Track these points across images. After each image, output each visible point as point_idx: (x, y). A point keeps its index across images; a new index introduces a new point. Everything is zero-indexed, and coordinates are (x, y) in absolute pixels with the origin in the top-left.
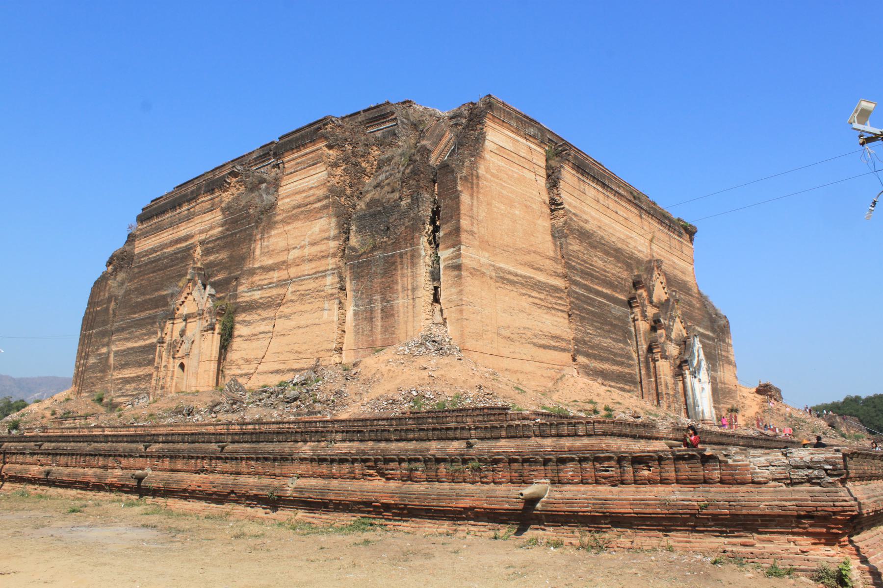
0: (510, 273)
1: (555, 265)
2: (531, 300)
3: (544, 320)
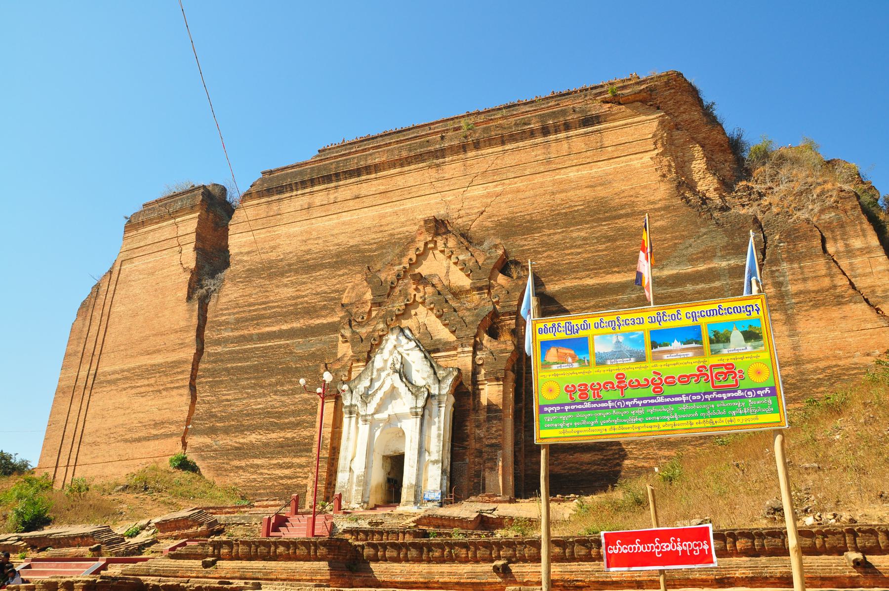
0: (114, 373)
2: (134, 391)
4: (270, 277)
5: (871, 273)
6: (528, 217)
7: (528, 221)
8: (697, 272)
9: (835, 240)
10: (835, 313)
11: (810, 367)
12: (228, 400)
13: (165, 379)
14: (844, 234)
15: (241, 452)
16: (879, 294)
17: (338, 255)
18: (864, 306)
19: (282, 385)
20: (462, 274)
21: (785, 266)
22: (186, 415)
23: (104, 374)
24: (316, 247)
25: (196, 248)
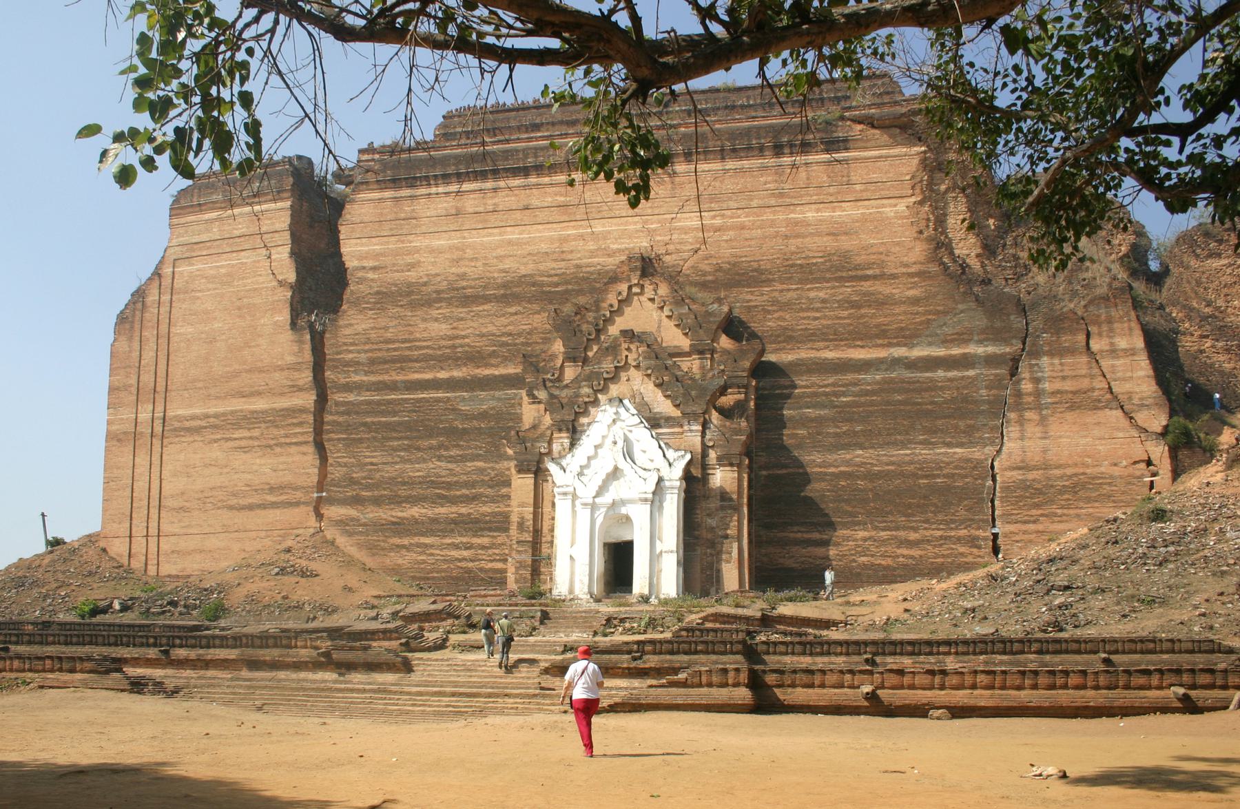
0: (193, 418)
1: (296, 375)
2: (231, 444)
3: (255, 467)
4: (413, 305)
5: (1131, 377)
6: (755, 265)
7: (755, 270)
8: (951, 356)
9: (1100, 334)
10: (1091, 418)
11: (1057, 472)
12: (372, 464)
13: (275, 432)
14: (1111, 330)
15: (399, 528)
16: (1136, 401)
17: (505, 285)
18: (1119, 413)
19: (447, 449)
20: (678, 332)
21: (1045, 360)
22: (315, 479)
23: (179, 419)
24: (474, 270)
25: (293, 253)
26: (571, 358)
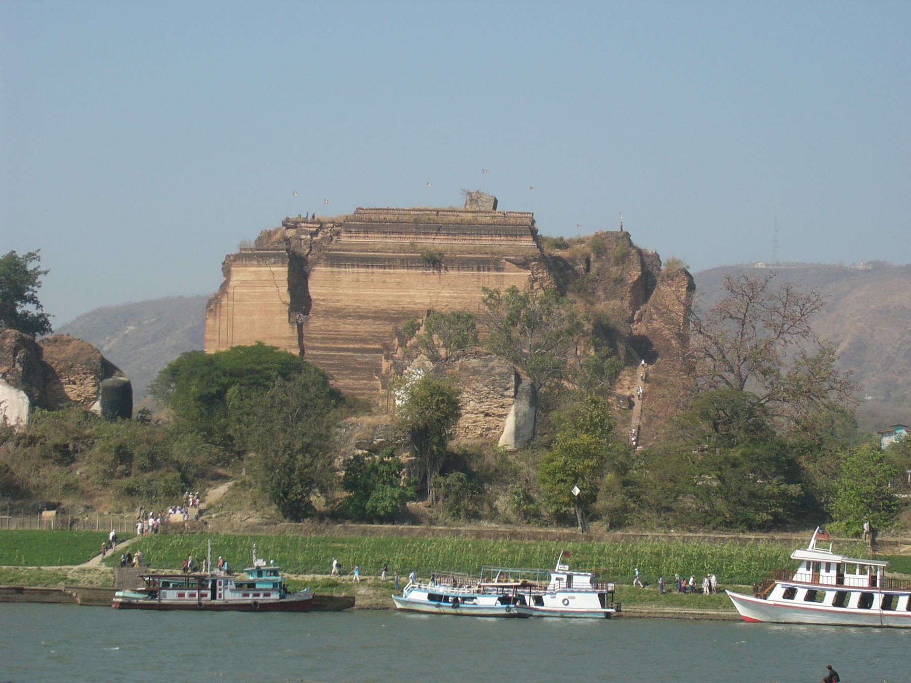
4: (340, 317)
17: (376, 312)
25: (289, 289)
26: (400, 345)
